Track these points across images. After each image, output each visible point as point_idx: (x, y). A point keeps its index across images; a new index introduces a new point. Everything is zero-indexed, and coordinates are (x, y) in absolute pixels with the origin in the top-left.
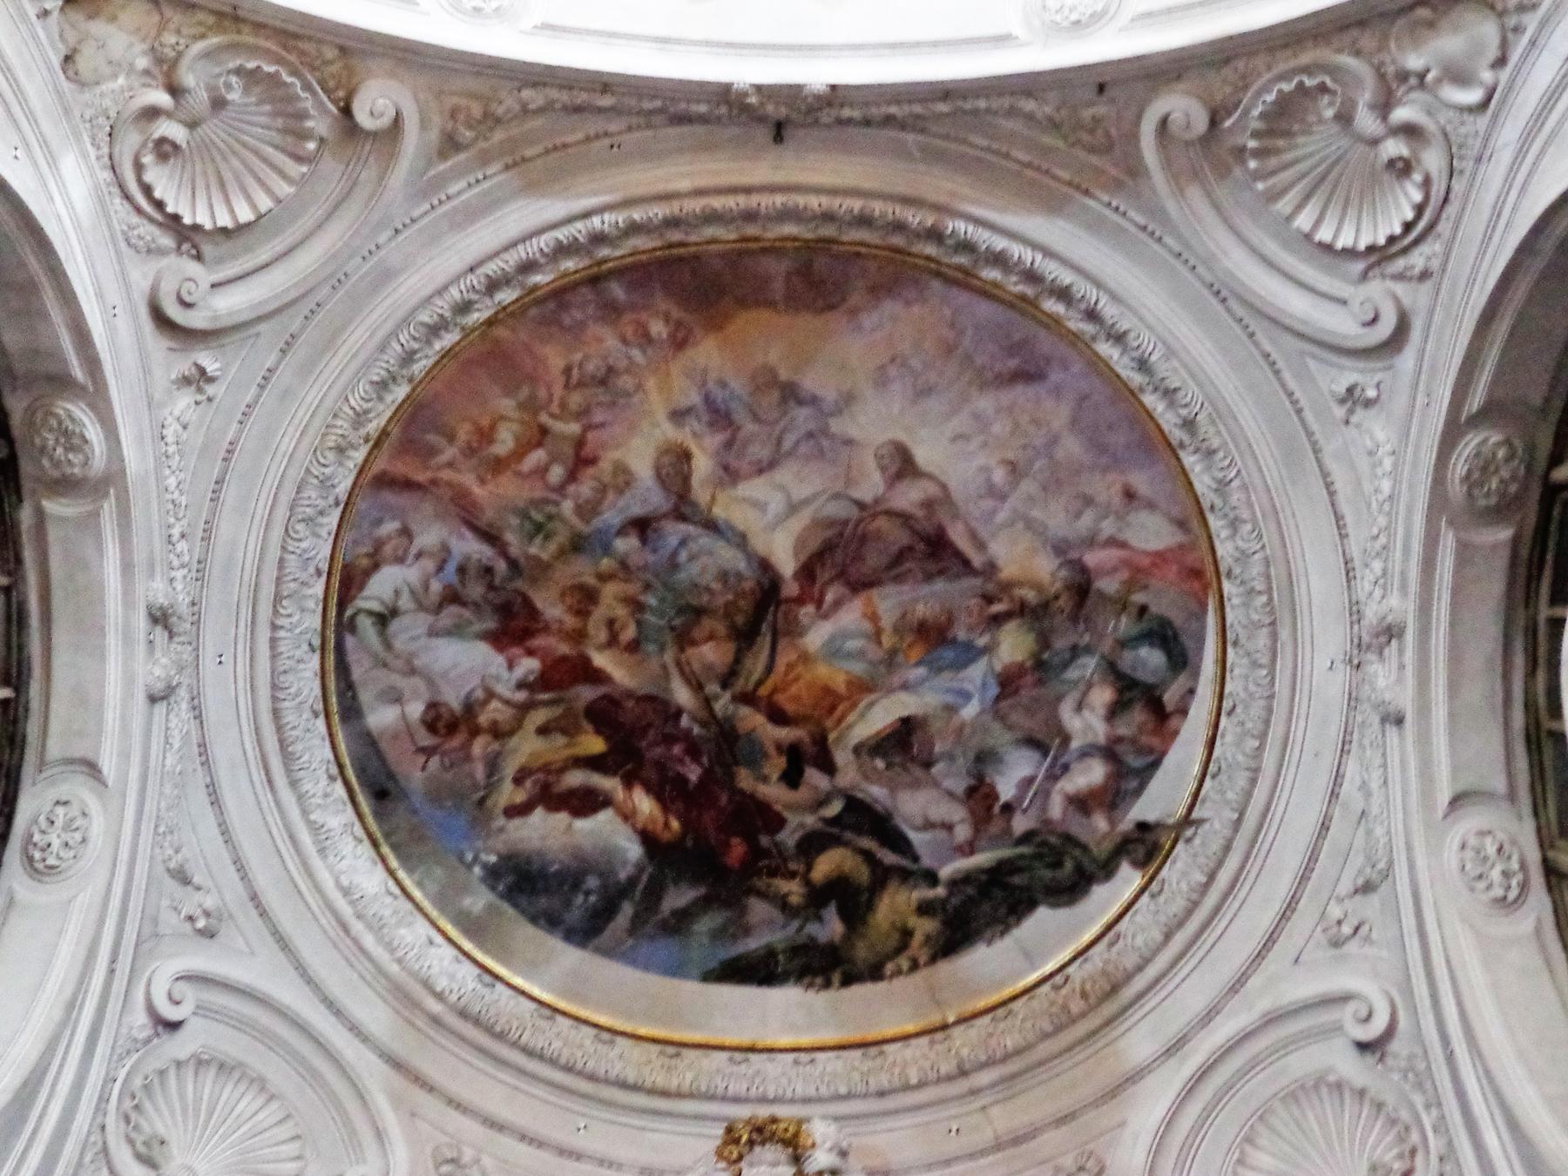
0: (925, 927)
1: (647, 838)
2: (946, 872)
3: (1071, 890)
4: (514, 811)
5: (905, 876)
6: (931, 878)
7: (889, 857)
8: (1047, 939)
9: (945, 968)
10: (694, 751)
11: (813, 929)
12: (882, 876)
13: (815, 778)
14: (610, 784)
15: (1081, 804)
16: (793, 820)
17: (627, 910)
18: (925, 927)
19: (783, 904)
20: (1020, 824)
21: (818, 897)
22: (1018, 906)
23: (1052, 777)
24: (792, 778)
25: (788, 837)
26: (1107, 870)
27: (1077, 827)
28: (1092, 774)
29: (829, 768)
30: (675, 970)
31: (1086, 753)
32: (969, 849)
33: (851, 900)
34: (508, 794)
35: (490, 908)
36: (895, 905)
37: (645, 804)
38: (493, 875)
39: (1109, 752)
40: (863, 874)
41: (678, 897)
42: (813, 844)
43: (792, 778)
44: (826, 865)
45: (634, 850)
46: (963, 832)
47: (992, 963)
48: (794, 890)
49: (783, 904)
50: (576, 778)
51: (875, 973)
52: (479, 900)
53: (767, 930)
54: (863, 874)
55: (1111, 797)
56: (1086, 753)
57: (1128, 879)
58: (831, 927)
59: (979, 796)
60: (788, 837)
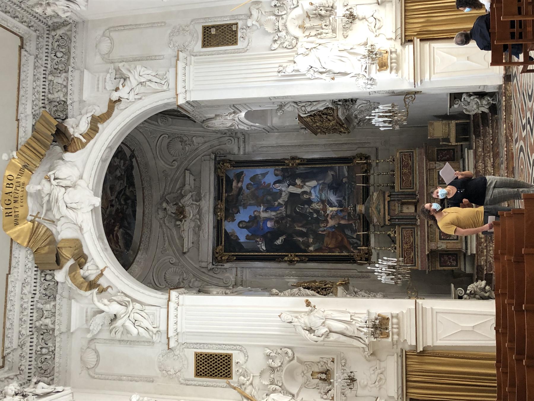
0: (131, 189)
1: (120, 228)
2: (125, 185)
3: (132, 167)
4: (120, 248)
5: (125, 190)
6: (126, 187)
7: (123, 192)
8: (135, 172)
9: (136, 186)
10: (111, 221)
11: (130, 204)
12: (124, 194)
13: (114, 202)
14: (115, 233)
15: (124, 164)
16: (117, 206)
17: (128, 231)
18: (131, 189)
19: (127, 208)
20: (123, 173)
21: (126, 204)
22: (132, 175)
23: (120, 168)
24: (112, 206)
25: (119, 207)
26: (132, 162)
27: (126, 165)
28: (122, 161)
29: (113, 200)
30: (134, 223)
31: (120, 162)
32: (124, 181)
33: (127, 199)
34: (118, 248)
35: (132, 250)
36: (128, 193)
37: (116, 228)
38: (128, 250)
39: (121, 159)
40: (124, 197)
41: (126, 224)
42: (120, 204)
43: (112, 206)
44: (123, 202)
45: (121, 230)
46: (122, 182)
47: (137, 181)
48: (125, 207)
49: (127, 208)
50: (115, 238)
51: (135, 196)
52: (131, 252)
53: (129, 211)
54: (124, 197)
55: (125, 160)
56: (120, 162)
57: (134, 160)
58: (129, 202)
59: (119, 178)
60: (119, 207)
